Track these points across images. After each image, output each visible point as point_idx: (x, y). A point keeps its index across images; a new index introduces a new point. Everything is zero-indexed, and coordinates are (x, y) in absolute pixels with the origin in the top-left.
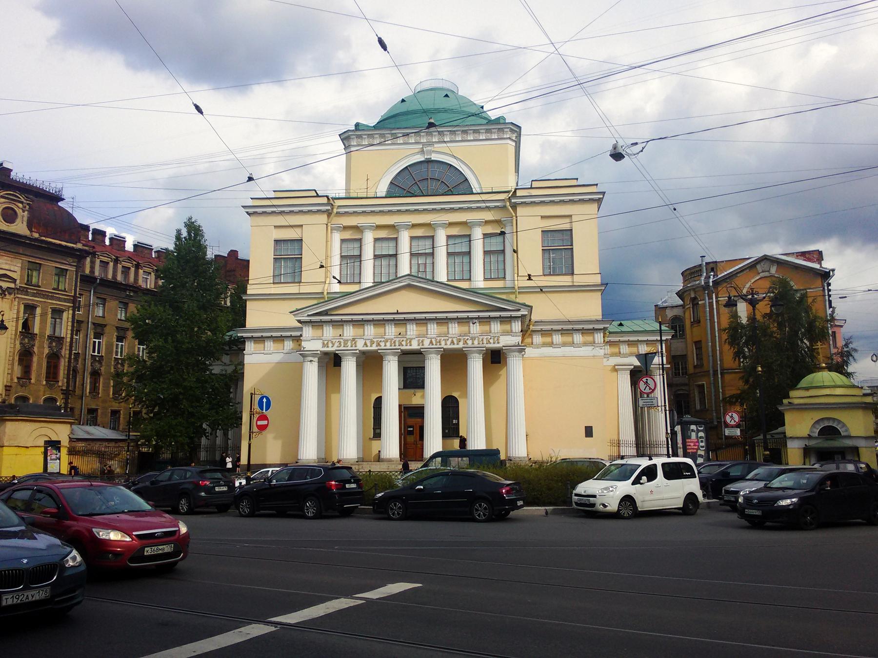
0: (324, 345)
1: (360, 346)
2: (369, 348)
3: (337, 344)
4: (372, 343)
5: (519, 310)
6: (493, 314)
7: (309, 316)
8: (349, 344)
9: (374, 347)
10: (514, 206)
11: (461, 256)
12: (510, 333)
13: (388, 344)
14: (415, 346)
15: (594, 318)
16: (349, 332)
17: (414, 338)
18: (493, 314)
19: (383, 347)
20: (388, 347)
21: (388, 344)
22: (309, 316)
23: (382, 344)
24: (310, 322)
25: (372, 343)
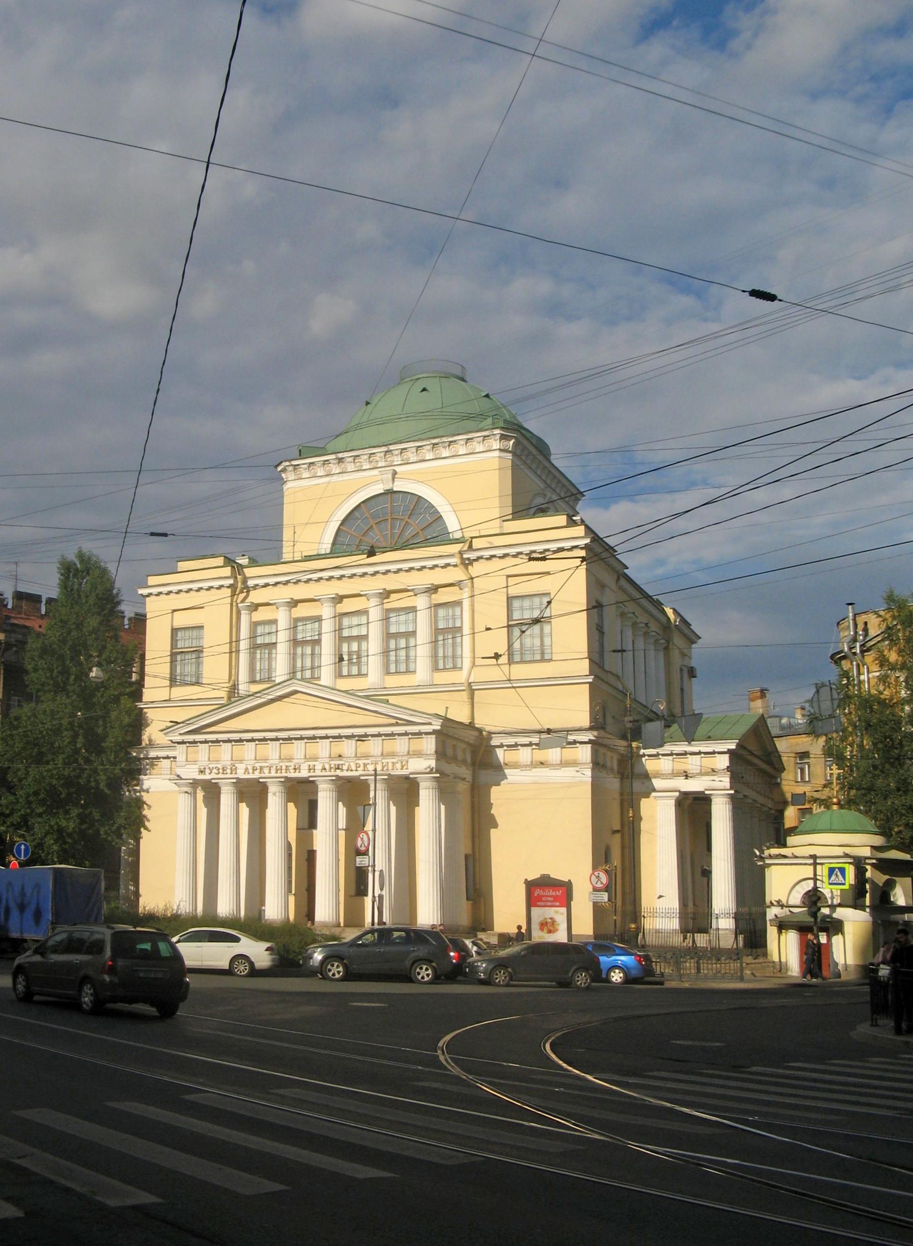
0: (202, 772)
1: (241, 774)
2: (251, 776)
3: (215, 771)
4: (254, 769)
5: (430, 724)
6: (397, 729)
7: (180, 734)
8: (229, 771)
9: (257, 775)
10: (467, 563)
11: (396, 642)
12: (419, 754)
13: (273, 771)
14: (304, 773)
15: (578, 725)
16: (225, 753)
17: (303, 761)
18: (397, 729)
19: (267, 775)
20: (273, 774)
21: (273, 771)
22: (180, 734)
23: (266, 771)
24: (183, 743)
25: (254, 769)
